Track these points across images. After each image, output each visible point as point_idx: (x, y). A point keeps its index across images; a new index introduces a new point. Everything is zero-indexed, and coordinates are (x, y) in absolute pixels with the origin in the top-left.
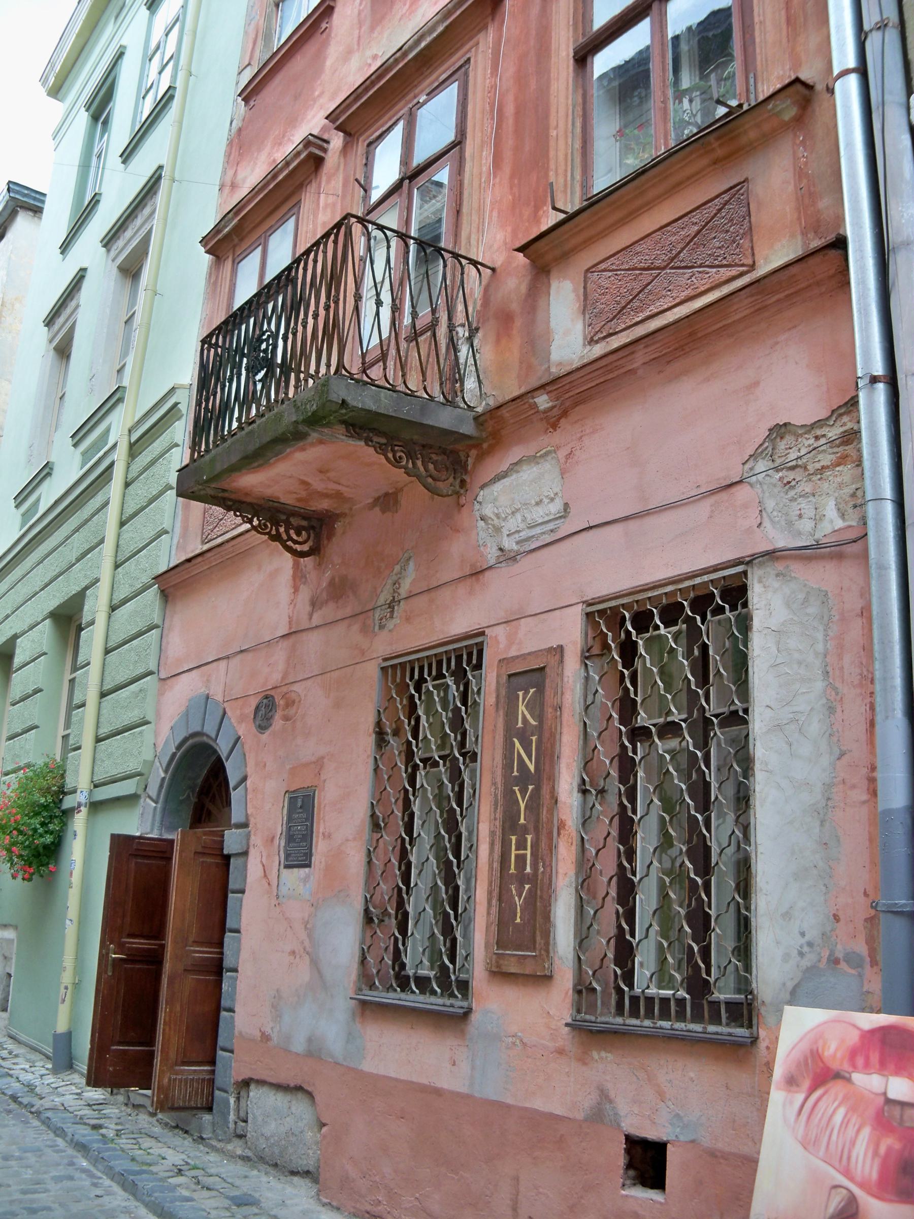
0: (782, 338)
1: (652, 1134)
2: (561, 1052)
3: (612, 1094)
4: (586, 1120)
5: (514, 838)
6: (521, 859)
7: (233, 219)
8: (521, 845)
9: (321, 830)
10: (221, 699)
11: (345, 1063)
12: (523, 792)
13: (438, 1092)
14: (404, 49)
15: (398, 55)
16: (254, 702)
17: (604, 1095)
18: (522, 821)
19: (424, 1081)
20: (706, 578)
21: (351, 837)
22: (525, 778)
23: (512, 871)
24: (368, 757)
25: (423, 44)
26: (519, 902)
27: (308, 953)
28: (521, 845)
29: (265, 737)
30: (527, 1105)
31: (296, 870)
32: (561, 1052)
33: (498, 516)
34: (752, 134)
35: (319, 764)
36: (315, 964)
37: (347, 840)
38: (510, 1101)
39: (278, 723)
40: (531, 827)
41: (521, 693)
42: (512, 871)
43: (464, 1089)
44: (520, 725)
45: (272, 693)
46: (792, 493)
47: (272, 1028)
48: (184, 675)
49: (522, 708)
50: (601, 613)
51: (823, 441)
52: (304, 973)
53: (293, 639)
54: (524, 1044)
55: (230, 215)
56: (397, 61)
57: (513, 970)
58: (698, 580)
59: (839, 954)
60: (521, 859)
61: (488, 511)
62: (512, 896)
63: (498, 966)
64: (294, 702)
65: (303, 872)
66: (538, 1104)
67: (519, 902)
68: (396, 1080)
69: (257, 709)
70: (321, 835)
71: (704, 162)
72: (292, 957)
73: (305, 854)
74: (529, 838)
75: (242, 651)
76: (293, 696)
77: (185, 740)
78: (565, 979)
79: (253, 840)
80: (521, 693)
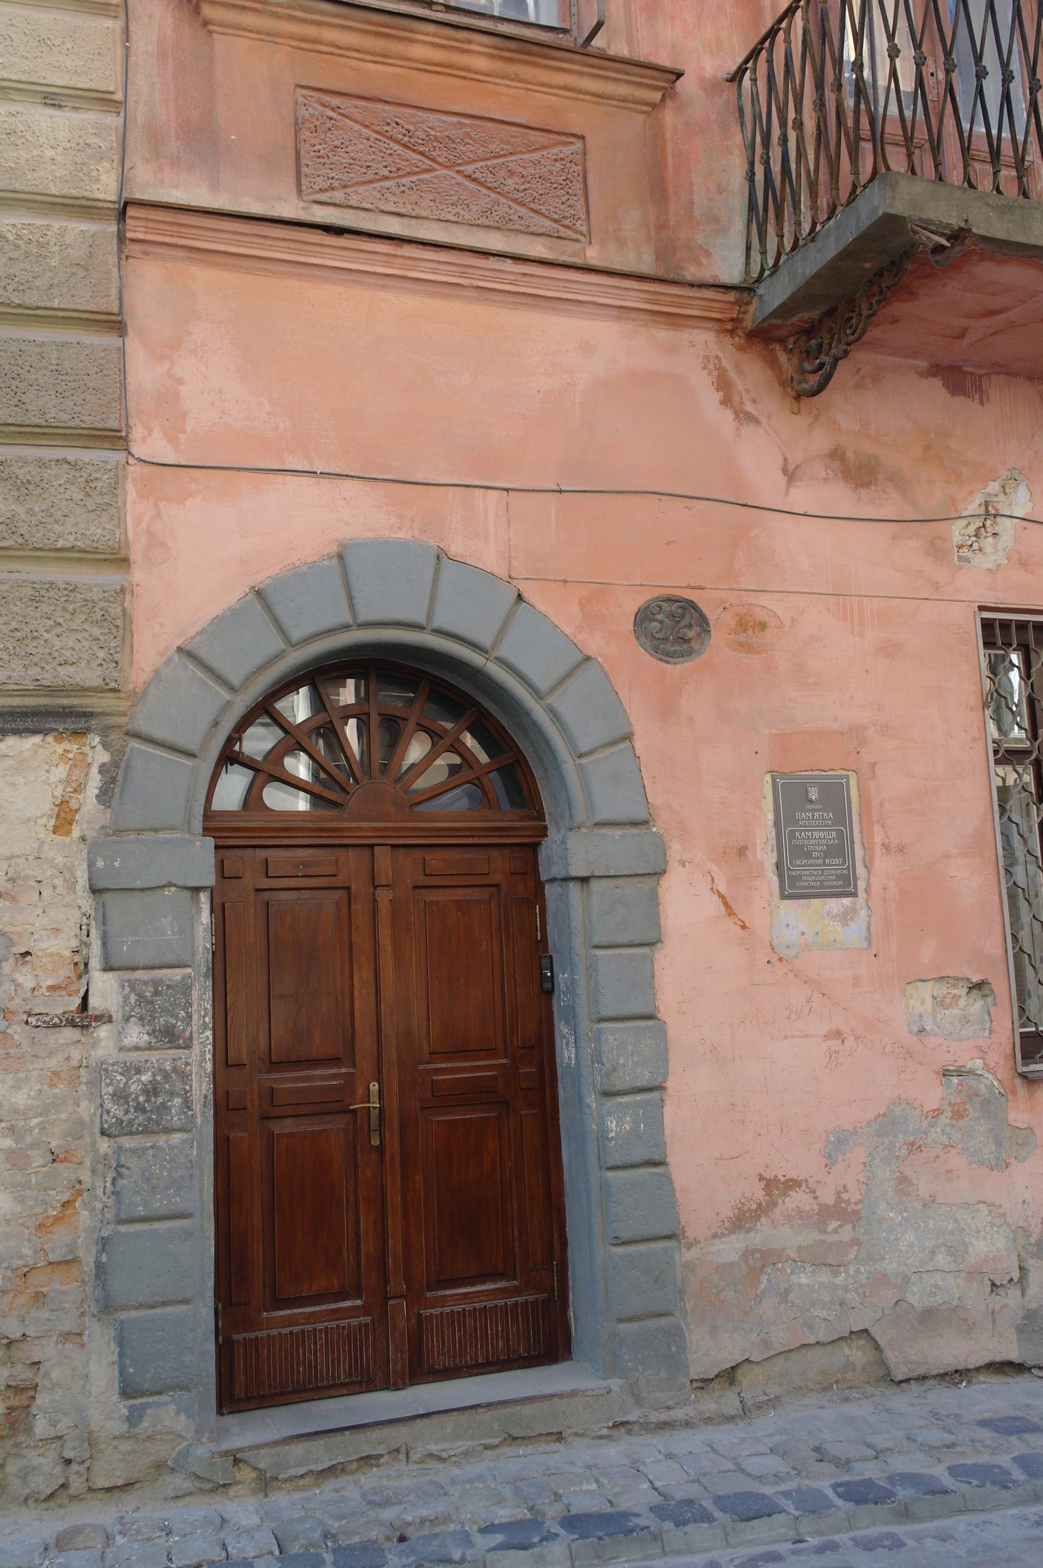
9: (878, 839)
10: (503, 573)
16: (631, 604)
24: (974, 740)
29: (675, 669)
31: (816, 902)
37: (947, 856)
48: (290, 479)
65: (835, 905)
69: (643, 617)
70: (878, 848)
72: (835, 1044)
73: (839, 877)
76: (759, 614)
77: (345, 627)
79: (675, 850)
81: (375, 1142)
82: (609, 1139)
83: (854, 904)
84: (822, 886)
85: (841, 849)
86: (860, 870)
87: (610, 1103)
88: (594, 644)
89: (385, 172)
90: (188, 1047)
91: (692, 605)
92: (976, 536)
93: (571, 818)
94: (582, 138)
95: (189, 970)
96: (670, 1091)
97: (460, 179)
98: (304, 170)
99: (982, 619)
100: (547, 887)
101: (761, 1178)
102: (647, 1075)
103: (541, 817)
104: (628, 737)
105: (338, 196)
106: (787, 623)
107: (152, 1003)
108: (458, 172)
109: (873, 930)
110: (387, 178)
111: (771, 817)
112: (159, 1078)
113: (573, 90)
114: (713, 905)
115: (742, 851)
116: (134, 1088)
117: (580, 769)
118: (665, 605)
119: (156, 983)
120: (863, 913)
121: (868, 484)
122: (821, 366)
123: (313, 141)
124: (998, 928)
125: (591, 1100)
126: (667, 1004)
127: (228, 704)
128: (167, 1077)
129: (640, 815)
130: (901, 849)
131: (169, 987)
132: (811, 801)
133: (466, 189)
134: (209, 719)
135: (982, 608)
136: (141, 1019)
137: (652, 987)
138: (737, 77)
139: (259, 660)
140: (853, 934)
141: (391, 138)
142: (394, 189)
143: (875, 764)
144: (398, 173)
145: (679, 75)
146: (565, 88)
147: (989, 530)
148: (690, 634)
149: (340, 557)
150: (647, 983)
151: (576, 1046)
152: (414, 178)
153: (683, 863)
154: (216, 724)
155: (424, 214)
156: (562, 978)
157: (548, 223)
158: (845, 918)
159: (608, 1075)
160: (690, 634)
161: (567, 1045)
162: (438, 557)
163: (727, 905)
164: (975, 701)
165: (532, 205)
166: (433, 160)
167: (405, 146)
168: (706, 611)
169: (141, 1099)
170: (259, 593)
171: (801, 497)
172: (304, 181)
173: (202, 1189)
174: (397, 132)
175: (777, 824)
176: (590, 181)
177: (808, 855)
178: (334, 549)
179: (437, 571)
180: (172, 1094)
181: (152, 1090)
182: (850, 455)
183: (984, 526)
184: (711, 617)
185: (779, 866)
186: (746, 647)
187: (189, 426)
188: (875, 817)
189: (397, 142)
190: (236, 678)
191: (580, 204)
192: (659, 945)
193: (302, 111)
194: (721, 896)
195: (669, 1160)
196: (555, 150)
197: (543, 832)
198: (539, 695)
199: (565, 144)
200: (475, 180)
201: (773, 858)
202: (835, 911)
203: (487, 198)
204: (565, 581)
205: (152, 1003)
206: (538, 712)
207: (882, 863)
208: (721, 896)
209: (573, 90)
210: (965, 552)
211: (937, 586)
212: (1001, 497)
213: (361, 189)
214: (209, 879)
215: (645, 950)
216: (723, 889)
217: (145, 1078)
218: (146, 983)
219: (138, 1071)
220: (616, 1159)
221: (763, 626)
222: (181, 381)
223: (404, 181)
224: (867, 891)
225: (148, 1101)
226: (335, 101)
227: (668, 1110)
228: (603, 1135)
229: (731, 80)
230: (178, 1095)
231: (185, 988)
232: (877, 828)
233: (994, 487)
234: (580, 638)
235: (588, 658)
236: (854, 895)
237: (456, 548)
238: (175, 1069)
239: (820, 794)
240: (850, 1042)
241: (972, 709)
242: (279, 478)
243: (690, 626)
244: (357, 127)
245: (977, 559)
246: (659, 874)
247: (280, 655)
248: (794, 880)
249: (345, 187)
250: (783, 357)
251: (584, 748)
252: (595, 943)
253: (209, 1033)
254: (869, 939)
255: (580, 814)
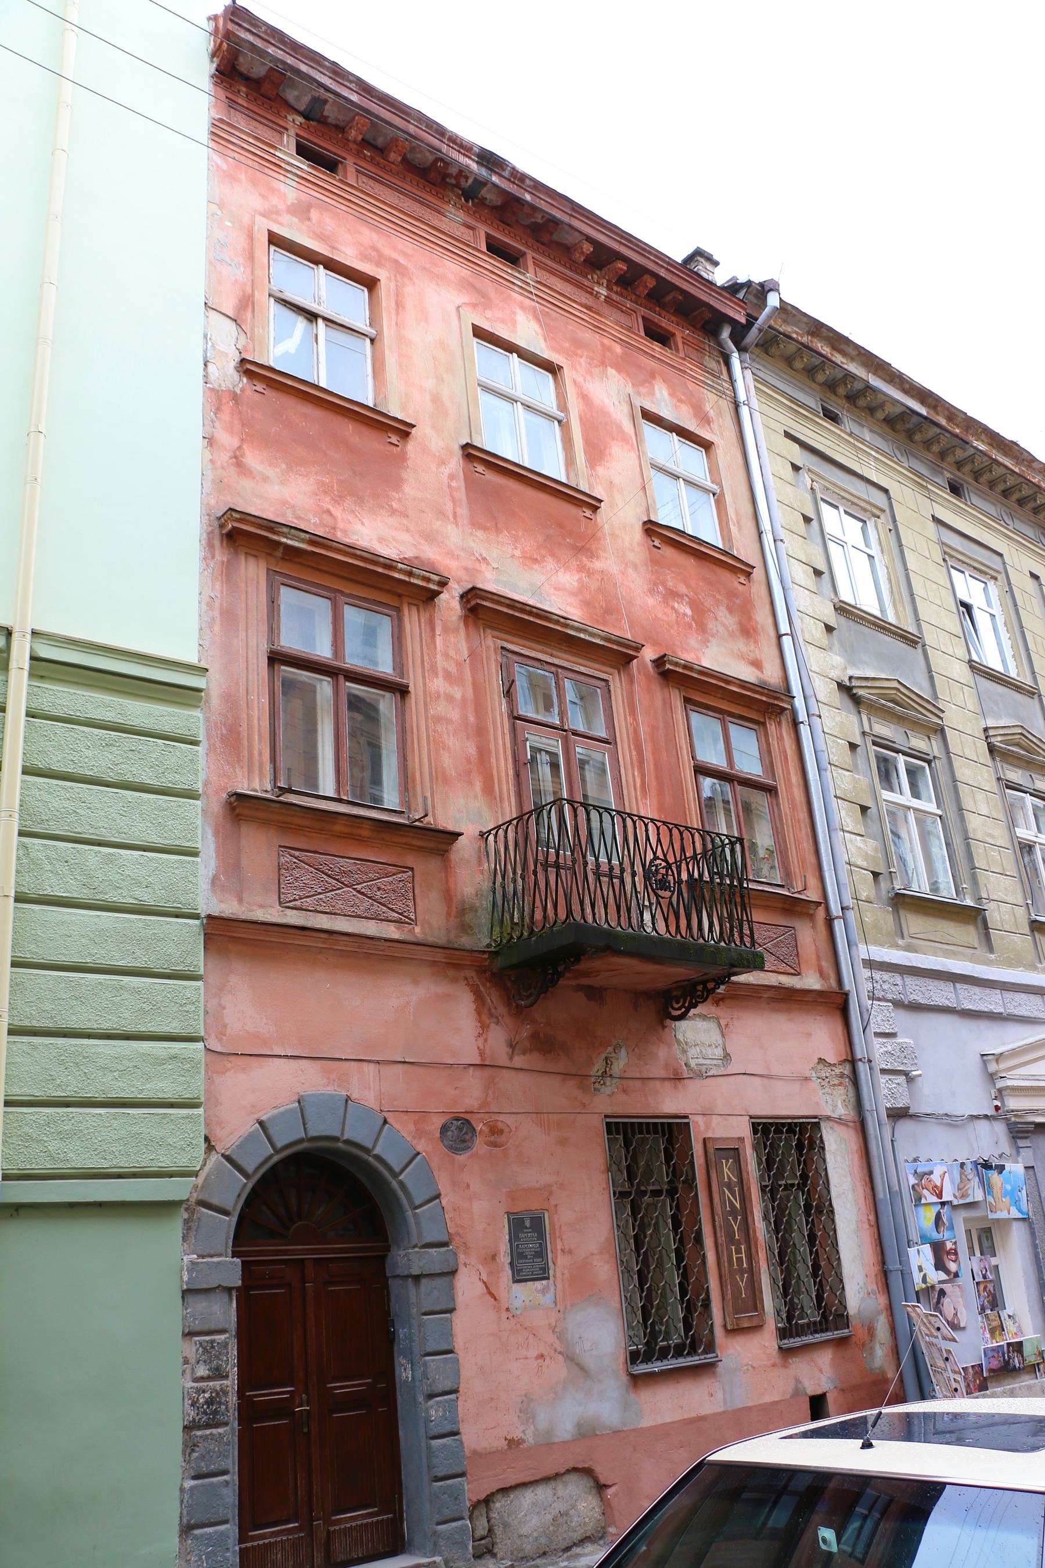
0: (818, 1018)
1: (819, 1392)
2: (774, 1365)
3: (801, 1379)
4: (791, 1398)
5: (733, 1247)
6: (739, 1260)
7: (303, 541)
8: (739, 1251)
9: (559, 1247)
11: (625, 1429)
12: (735, 1220)
13: (702, 1419)
14: (569, 622)
15: (562, 620)
16: (437, 1122)
17: (798, 1381)
18: (737, 1237)
19: (693, 1415)
20: (804, 1120)
21: (595, 1252)
22: (733, 1211)
23: (735, 1267)
24: (604, 1189)
25: (582, 636)
26: (742, 1285)
27: (560, 1353)
28: (739, 1251)
29: (462, 1158)
30: (761, 1402)
32: (774, 1365)
33: (686, 1043)
34: (799, 909)
35: (548, 1190)
36: (571, 1359)
37: (592, 1254)
38: (750, 1404)
39: (479, 1146)
40: (742, 1240)
41: (724, 1161)
42: (735, 1267)
43: (721, 1410)
44: (726, 1180)
45: (467, 1117)
46: (824, 1091)
47: (524, 1432)
48: (276, 1060)
49: (726, 1170)
50: (759, 1124)
51: (833, 1073)
52: (559, 1369)
53: (488, 1072)
54: (754, 1368)
55: (303, 535)
56: (557, 622)
57: (746, 1325)
58: (801, 1120)
59: (870, 1291)
60: (739, 1260)
61: (680, 1037)
62: (738, 1283)
63: (738, 1325)
64: (501, 1132)
65: (539, 1285)
66: (767, 1399)
67: (742, 1285)
68: (672, 1423)
69: (444, 1129)
70: (559, 1252)
71: (780, 905)
72: (541, 1361)
73: (541, 1269)
74: (743, 1247)
75: (405, 1062)
76: (500, 1125)
77: (301, 1141)
78: (771, 1324)
79: (462, 1258)
80: (724, 1161)
81: (306, 1430)
82: (432, 1421)
83: (548, 1283)
84: (532, 1275)
85: (541, 1254)
86: (550, 1264)
87: (431, 1403)
88: (421, 1146)
89: (320, 891)
90: (226, 1377)
91: (467, 1121)
92: (603, 1077)
93: (409, 1242)
94: (412, 869)
95: (227, 1335)
96: (461, 1392)
97: (355, 893)
98: (282, 890)
99: (607, 1123)
100: (390, 1280)
101: (506, 1439)
102: (450, 1384)
103: (387, 1240)
104: (438, 1196)
105: (298, 903)
106: (514, 1129)
107: (210, 1353)
108: (354, 889)
109: (558, 1297)
110: (320, 893)
111: (507, 1237)
112: (214, 1395)
113: (409, 845)
114: (480, 1288)
115: (494, 1257)
116: (201, 1401)
117: (415, 1215)
118: (455, 1122)
119: (212, 1342)
120: (552, 1288)
121: (550, 1052)
122: (531, 995)
123: (287, 875)
124: (617, 1292)
125: (421, 1399)
126: (459, 1343)
127: (245, 1185)
128: (218, 1394)
129: (444, 1238)
130: (570, 1252)
131: (218, 1343)
132: (526, 1228)
133: (358, 898)
134: (237, 1193)
135: (606, 1116)
136: (205, 1362)
137: (451, 1335)
138: (483, 836)
139: (261, 1159)
140: (547, 1300)
141: (323, 872)
142: (325, 900)
143: (556, 1206)
144: (326, 891)
145: (461, 834)
146: (405, 844)
147: (608, 1073)
148: (467, 1137)
149: (299, 1102)
150: (448, 1333)
151: (412, 1370)
152: (333, 893)
153: (465, 1265)
154: (239, 1196)
155: (339, 912)
156: (402, 1333)
157: (396, 915)
158: (544, 1291)
159: (430, 1385)
160: (467, 1137)
161: (405, 1369)
162: (347, 1101)
163: (487, 1287)
164: (603, 1168)
165: (389, 906)
166: (342, 883)
167: (329, 876)
168: (475, 1126)
169: (205, 1407)
170: (261, 1123)
171: (519, 1061)
172: (282, 896)
173: (233, 1457)
174: (324, 868)
175: (510, 1241)
176: (416, 892)
177: (526, 1257)
178: (296, 1098)
179: (346, 1107)
180: (220, 1403)
181: (210, 1402)
182: (542, 1035)
183: (606, 1071)
184: (479, 1127)
185: (511, 1264)
186: (495, 1145)
187: (228, 1033)
188: (557, 1235)
189: (326, 874)
190: (250, 1169)
191: (411, 904)
192: (455, 1312)
193: (282, 860)
194: (484, 1283)
195: (461, 1431)
196: (399, 876)
197: (388, 1249)
198: (396, 1175)
199: (404, 872)
200: (362, 894)
201: (509, 1261)
202: (539, 1288)
203: (368, 902)
204: (407, 1112)
205: (210, 1353)
206: (394, 1184)
207: (561, 1260)
208: (484, 1283)
209: (409, 845)
210: (597, 1086)
211: (584, 1106)
212: (613, 1055)
213: (308, 900)
214: (239, 1283)
215: (448, 1315)
216: (485, 1279)
217: (207, 1395)
218: (207, 1342)
219: (204, 1392)
220: (436, 1431)
221: (501, 1132)
222: (224, 1008)
223: (328, 894)
224: (554, 1276)
225: (208, 1408)
226: (297, 853)
227: (460, 1403)
228: (428, 1420)
229: (482, 834)
230: (224, 1404)
231: (225, 1345)
232: (558, 1241)
233: (610, 1049)
234: (415, 1142)
235: (418, 1153)
236: (548, 1278)
237: (354, 1096)
238: (221, 1389)
239: (531, 1222)
240: (548, 1359)
241: (603, 1172)
242: (271, 1060)
243: (466, 1133)
244: (307, 867)
245: (603, 1089)
246: (453, 1273)
247: (270, 1157)
248: (519, 1271)
249: (301, 899)
250: (509, 984)
251: (417, 1202)
252: (424, 1310)
253: (236, 1369)
254: (555, 1303)
255: (414, 1240)
